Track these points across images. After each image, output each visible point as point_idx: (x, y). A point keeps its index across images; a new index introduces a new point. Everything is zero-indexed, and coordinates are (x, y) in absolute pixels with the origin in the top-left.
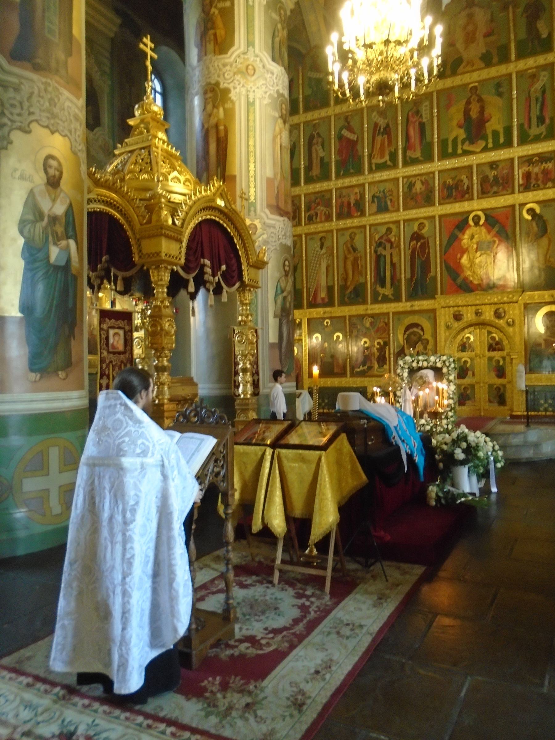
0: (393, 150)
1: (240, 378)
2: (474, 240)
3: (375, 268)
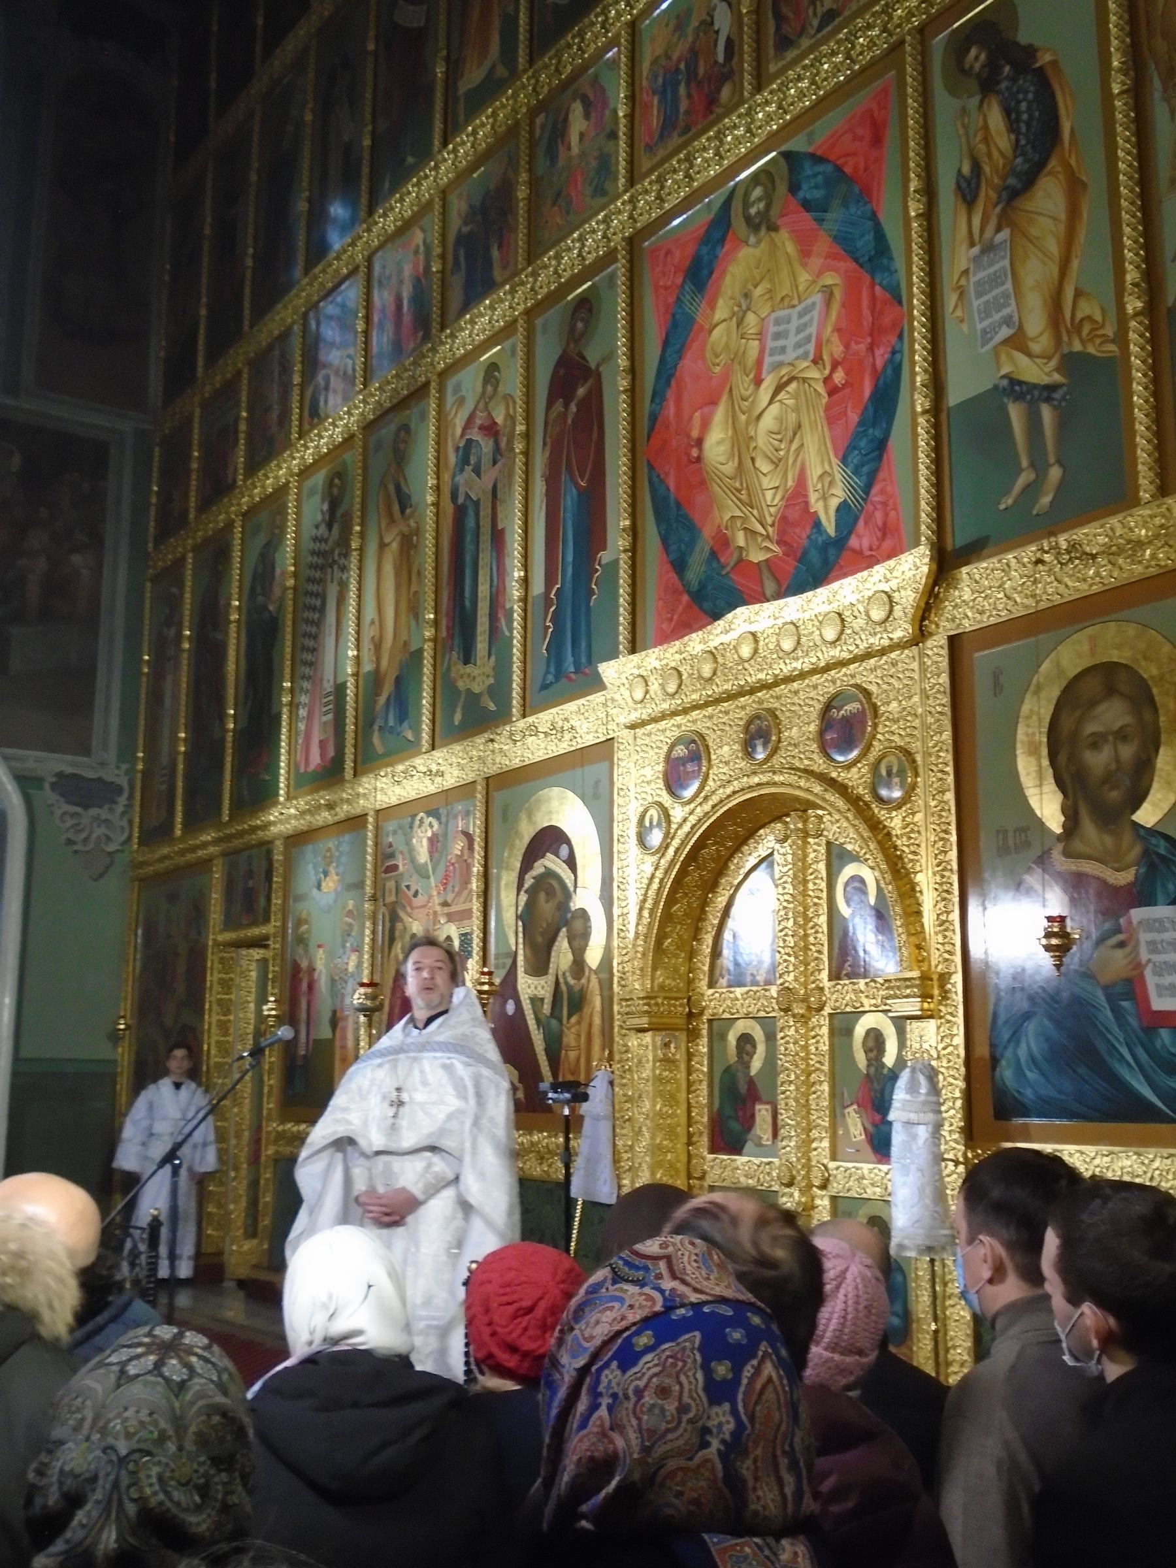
0: (510, 9)
2: (751, 318)
3: (450, 576)
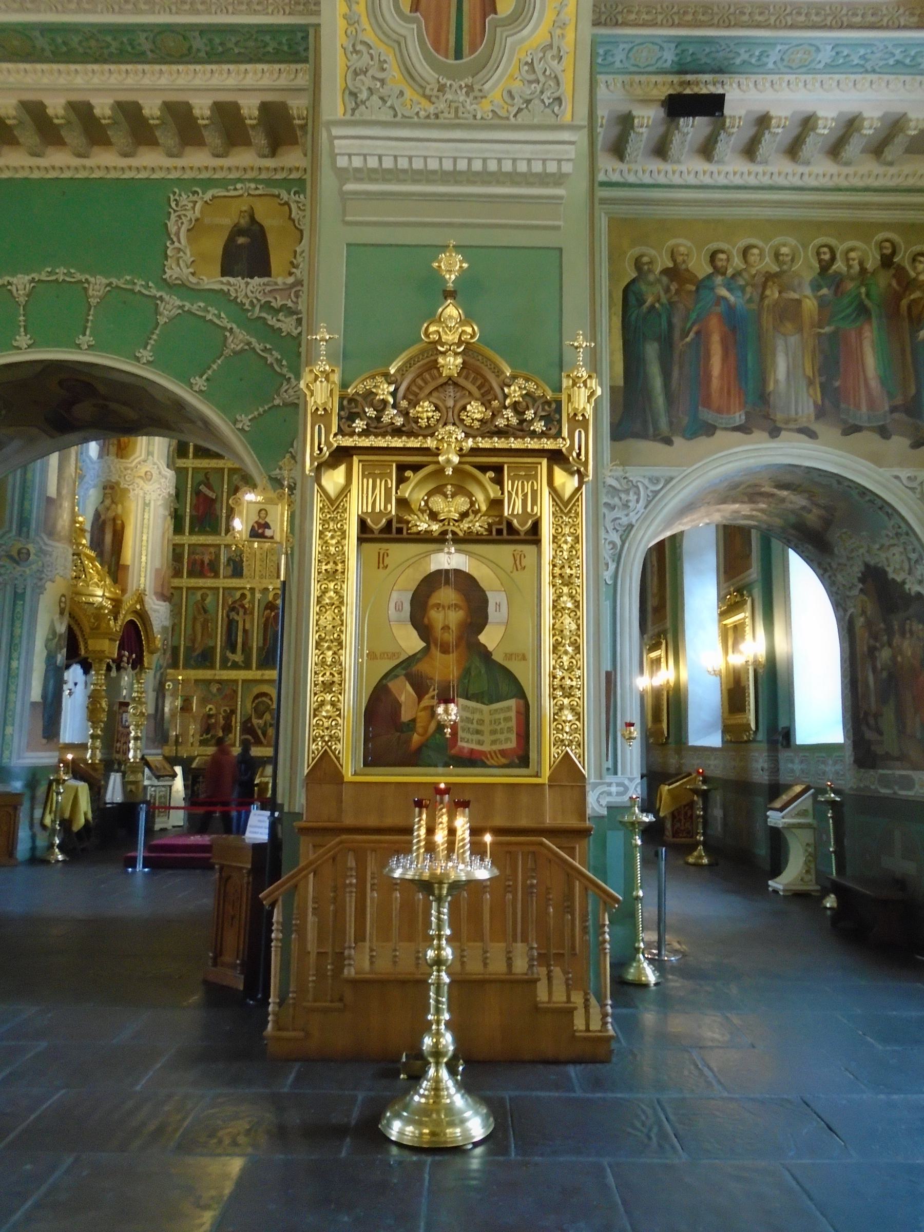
1: (131, 745)
